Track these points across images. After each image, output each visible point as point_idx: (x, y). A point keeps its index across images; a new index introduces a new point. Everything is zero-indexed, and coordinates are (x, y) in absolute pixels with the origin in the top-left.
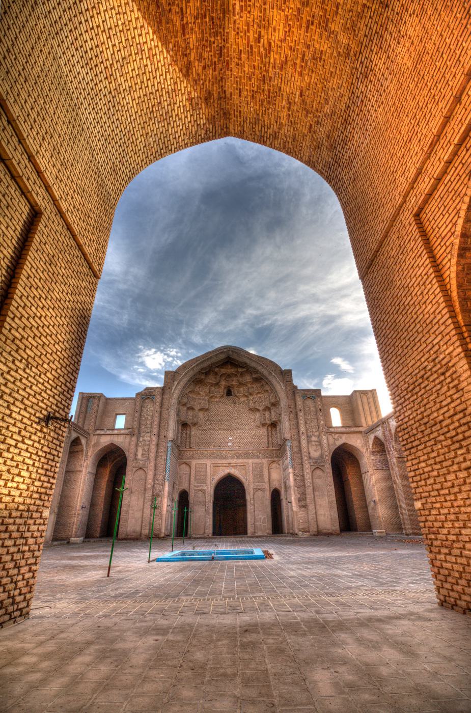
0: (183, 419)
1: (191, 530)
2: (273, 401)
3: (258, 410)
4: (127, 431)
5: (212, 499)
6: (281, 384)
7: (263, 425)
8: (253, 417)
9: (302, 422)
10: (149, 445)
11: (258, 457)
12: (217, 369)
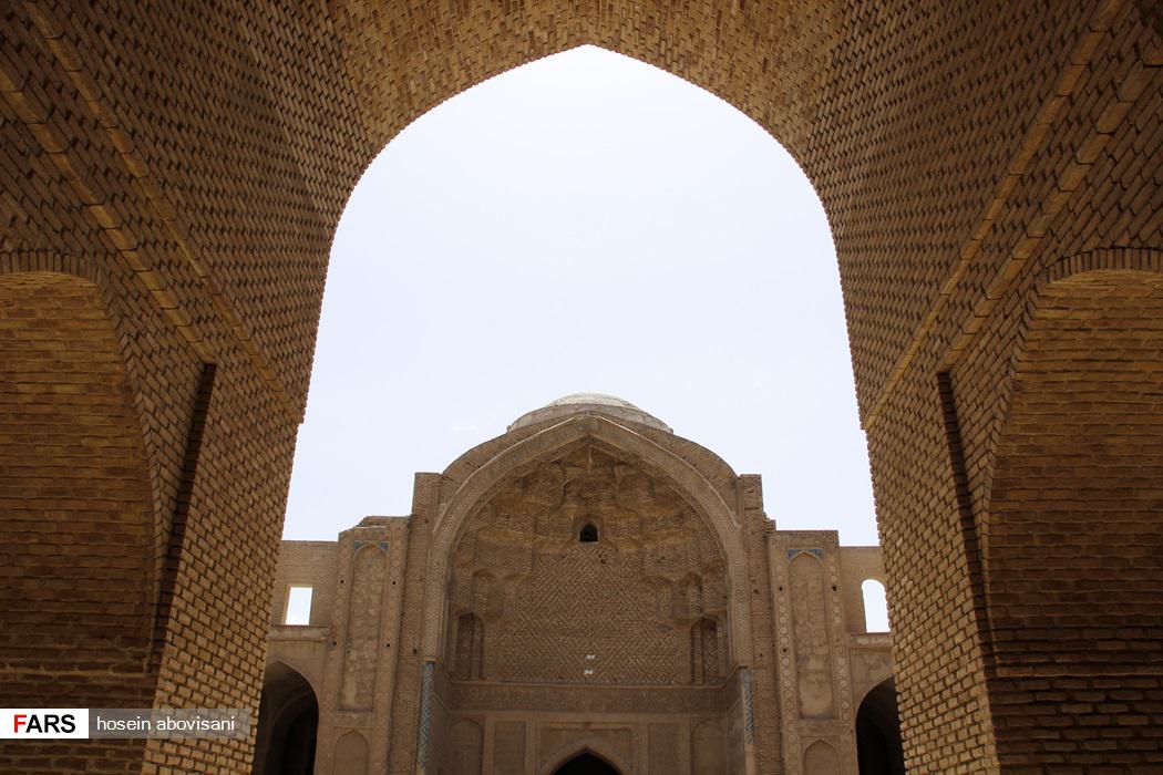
0: (464, 605)
2: (708, 558)
3: (668, 582)
4: (315, 633)
6: (732, 514)
7: (681, 623)
8: (653, 600)
9: (783, 620)
10: (375, 670)
12: (556, 470)
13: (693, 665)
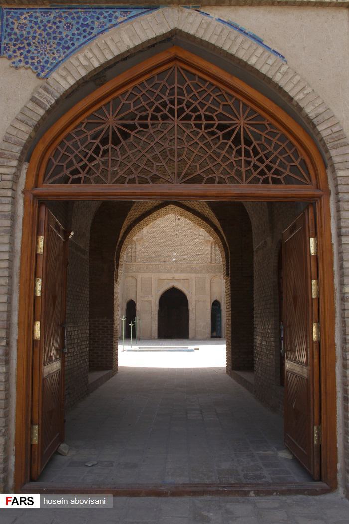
1: (137, 334)
5: (157, 308)
8: (197, 233)
11: (201, 272)
13: (211, 256)
